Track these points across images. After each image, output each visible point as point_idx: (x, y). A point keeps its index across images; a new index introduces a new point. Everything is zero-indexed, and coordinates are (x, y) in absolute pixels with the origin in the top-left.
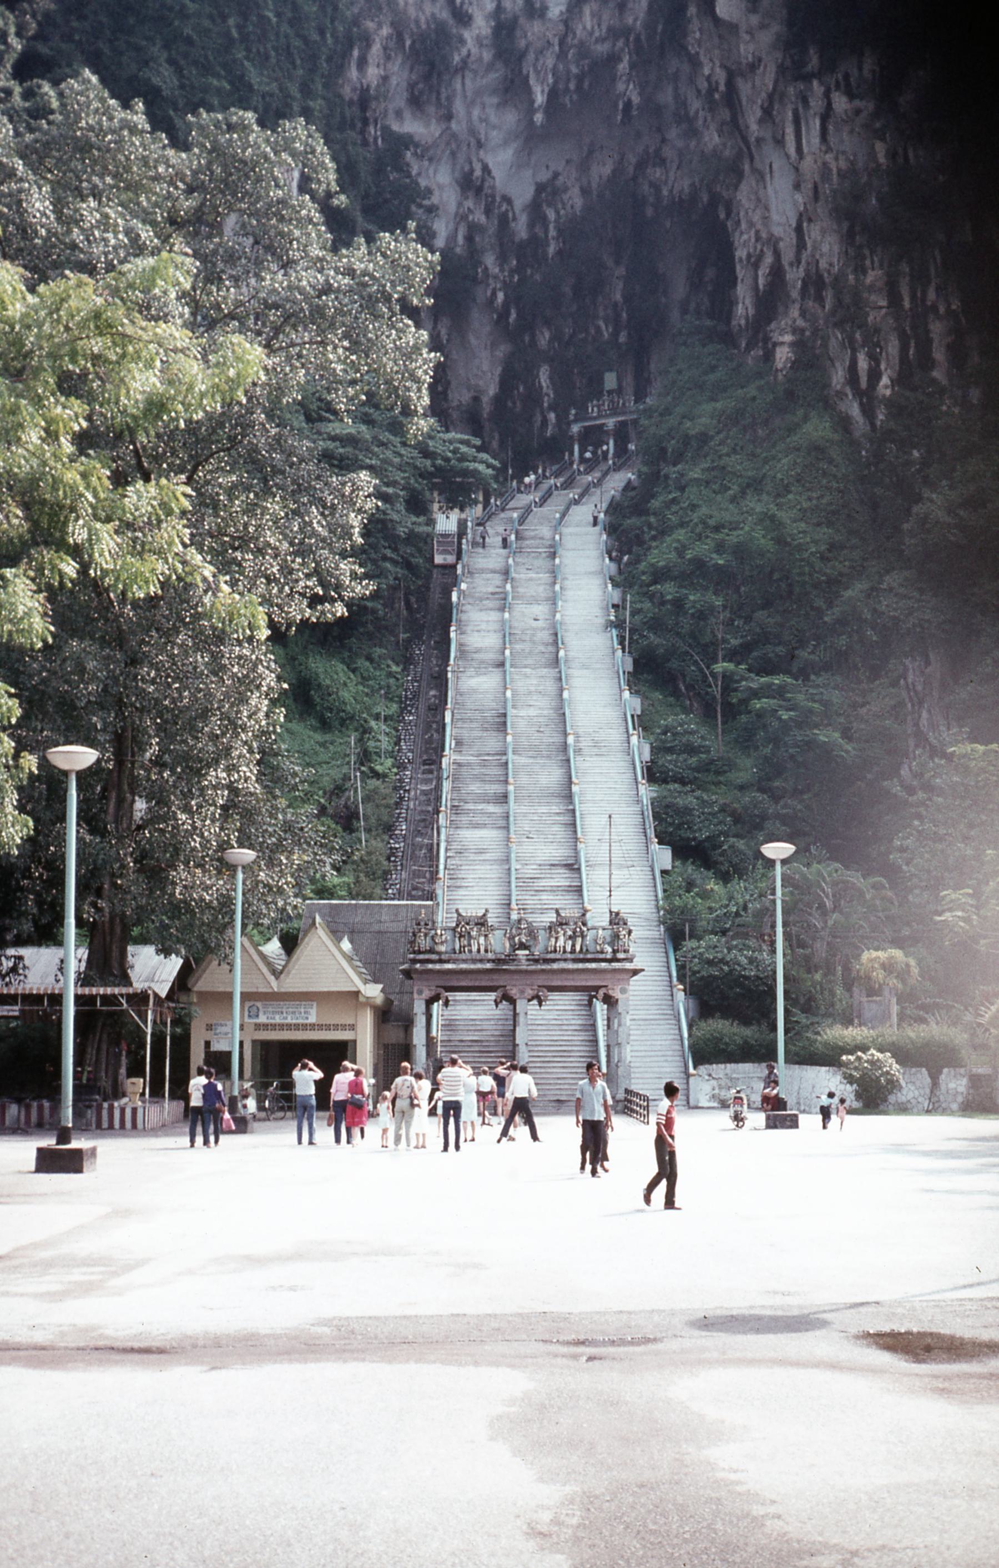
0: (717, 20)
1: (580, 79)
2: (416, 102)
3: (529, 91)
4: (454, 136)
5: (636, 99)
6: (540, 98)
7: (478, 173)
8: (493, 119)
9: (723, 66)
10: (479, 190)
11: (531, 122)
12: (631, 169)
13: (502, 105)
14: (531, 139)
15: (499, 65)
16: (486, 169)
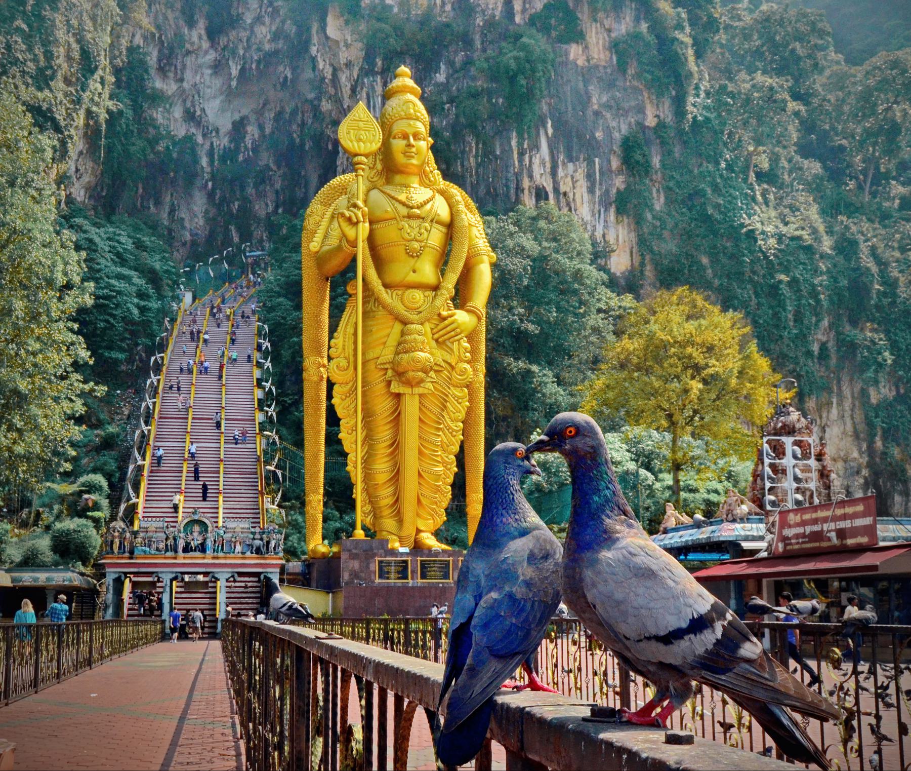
0: (327, 38)
1: (259, 62)
2: (162, 70)
3: (229, 68)
4: (184, 91)
5: (289, 75)
6: (235, 71)
7: (198, 113)
8: (208, 83)
9: (331, 65)
10: (198, 124)
11: (230, 86)
12: (287, 116)
13: (216, 73)
14: (230, 94)
15: (212, 51)
16: (203, 110)
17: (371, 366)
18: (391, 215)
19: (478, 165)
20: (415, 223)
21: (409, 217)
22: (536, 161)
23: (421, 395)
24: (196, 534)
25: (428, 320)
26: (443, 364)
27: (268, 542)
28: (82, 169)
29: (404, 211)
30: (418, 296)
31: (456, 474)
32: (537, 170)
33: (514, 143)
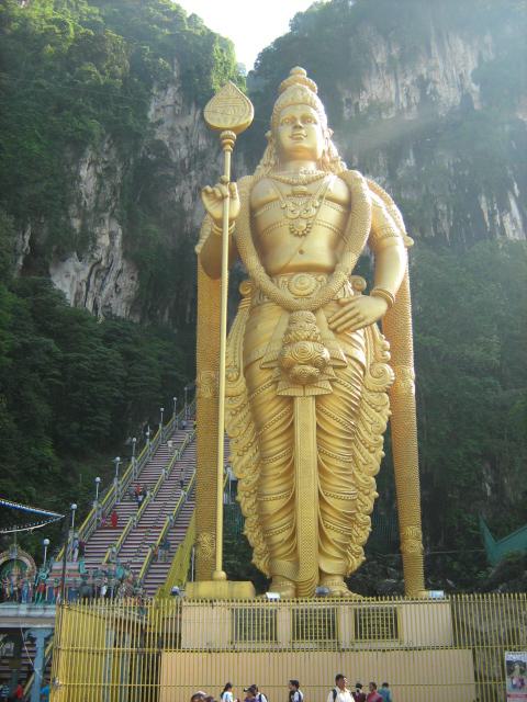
17: (256, 367)
18: (274, 196)
19: (451, 228)
20: (301, 201)
21: (294, 194)
22: (507, 219)
23: (318, 398)
24: (14, 579)
25: (323, 306)
26: (345, 359)
27: (100, 589)
28: (121, 285)
29: (287, 190)
30: (309, 282)
31: (376, 500)
32: (509, 227)
33: (484, 206)
